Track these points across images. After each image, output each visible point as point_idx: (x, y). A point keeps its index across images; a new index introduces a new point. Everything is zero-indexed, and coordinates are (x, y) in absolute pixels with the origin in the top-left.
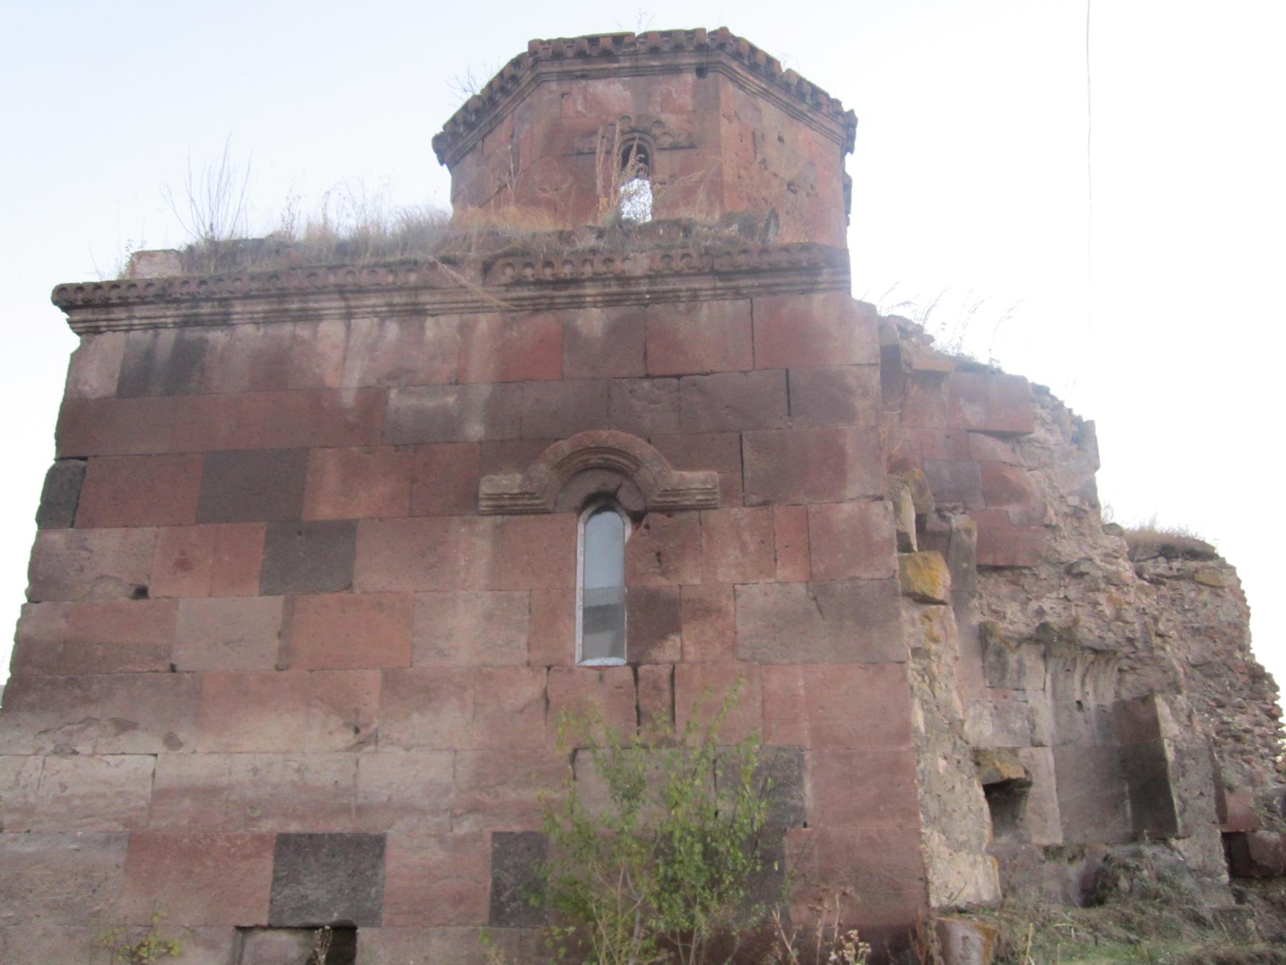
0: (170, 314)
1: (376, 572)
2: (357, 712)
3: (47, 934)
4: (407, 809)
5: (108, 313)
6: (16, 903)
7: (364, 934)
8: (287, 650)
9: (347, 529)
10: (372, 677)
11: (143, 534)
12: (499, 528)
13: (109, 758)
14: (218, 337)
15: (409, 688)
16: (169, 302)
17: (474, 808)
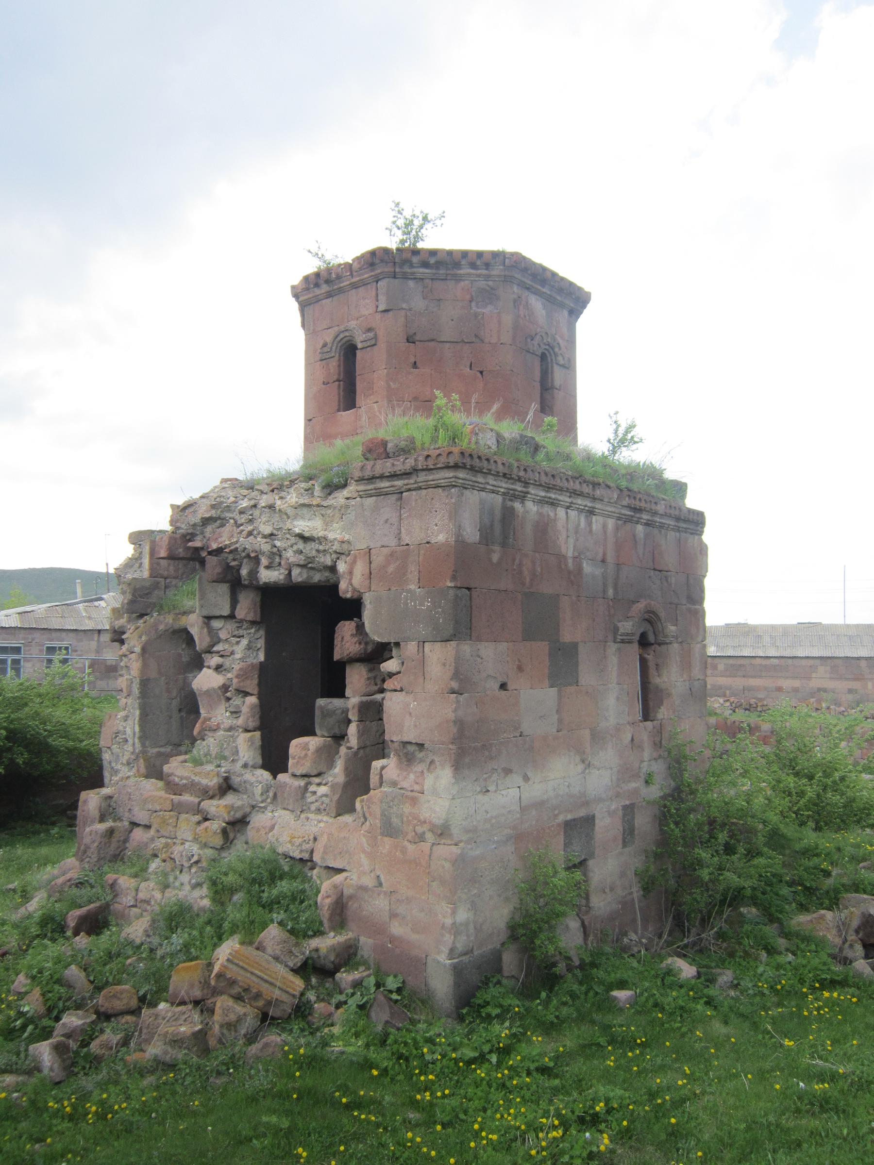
0: (504, 485)
1: (587, 677)
2: (584, 752)
3: (491, 898)
4: (600, 800)
5: (475, 476)
6: (477, 886)
7: (591, 863)
8: (560, 721)
9: (575, 646)
10: (587, 733)
11: (503, 646)
12: (619, 649)
13: (503, 792)
14: (517, 505)
15: (597, 737)
16: (509, 479)
17: (618, 795)
